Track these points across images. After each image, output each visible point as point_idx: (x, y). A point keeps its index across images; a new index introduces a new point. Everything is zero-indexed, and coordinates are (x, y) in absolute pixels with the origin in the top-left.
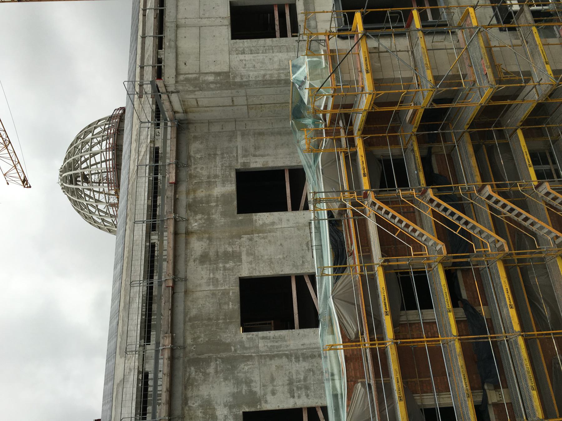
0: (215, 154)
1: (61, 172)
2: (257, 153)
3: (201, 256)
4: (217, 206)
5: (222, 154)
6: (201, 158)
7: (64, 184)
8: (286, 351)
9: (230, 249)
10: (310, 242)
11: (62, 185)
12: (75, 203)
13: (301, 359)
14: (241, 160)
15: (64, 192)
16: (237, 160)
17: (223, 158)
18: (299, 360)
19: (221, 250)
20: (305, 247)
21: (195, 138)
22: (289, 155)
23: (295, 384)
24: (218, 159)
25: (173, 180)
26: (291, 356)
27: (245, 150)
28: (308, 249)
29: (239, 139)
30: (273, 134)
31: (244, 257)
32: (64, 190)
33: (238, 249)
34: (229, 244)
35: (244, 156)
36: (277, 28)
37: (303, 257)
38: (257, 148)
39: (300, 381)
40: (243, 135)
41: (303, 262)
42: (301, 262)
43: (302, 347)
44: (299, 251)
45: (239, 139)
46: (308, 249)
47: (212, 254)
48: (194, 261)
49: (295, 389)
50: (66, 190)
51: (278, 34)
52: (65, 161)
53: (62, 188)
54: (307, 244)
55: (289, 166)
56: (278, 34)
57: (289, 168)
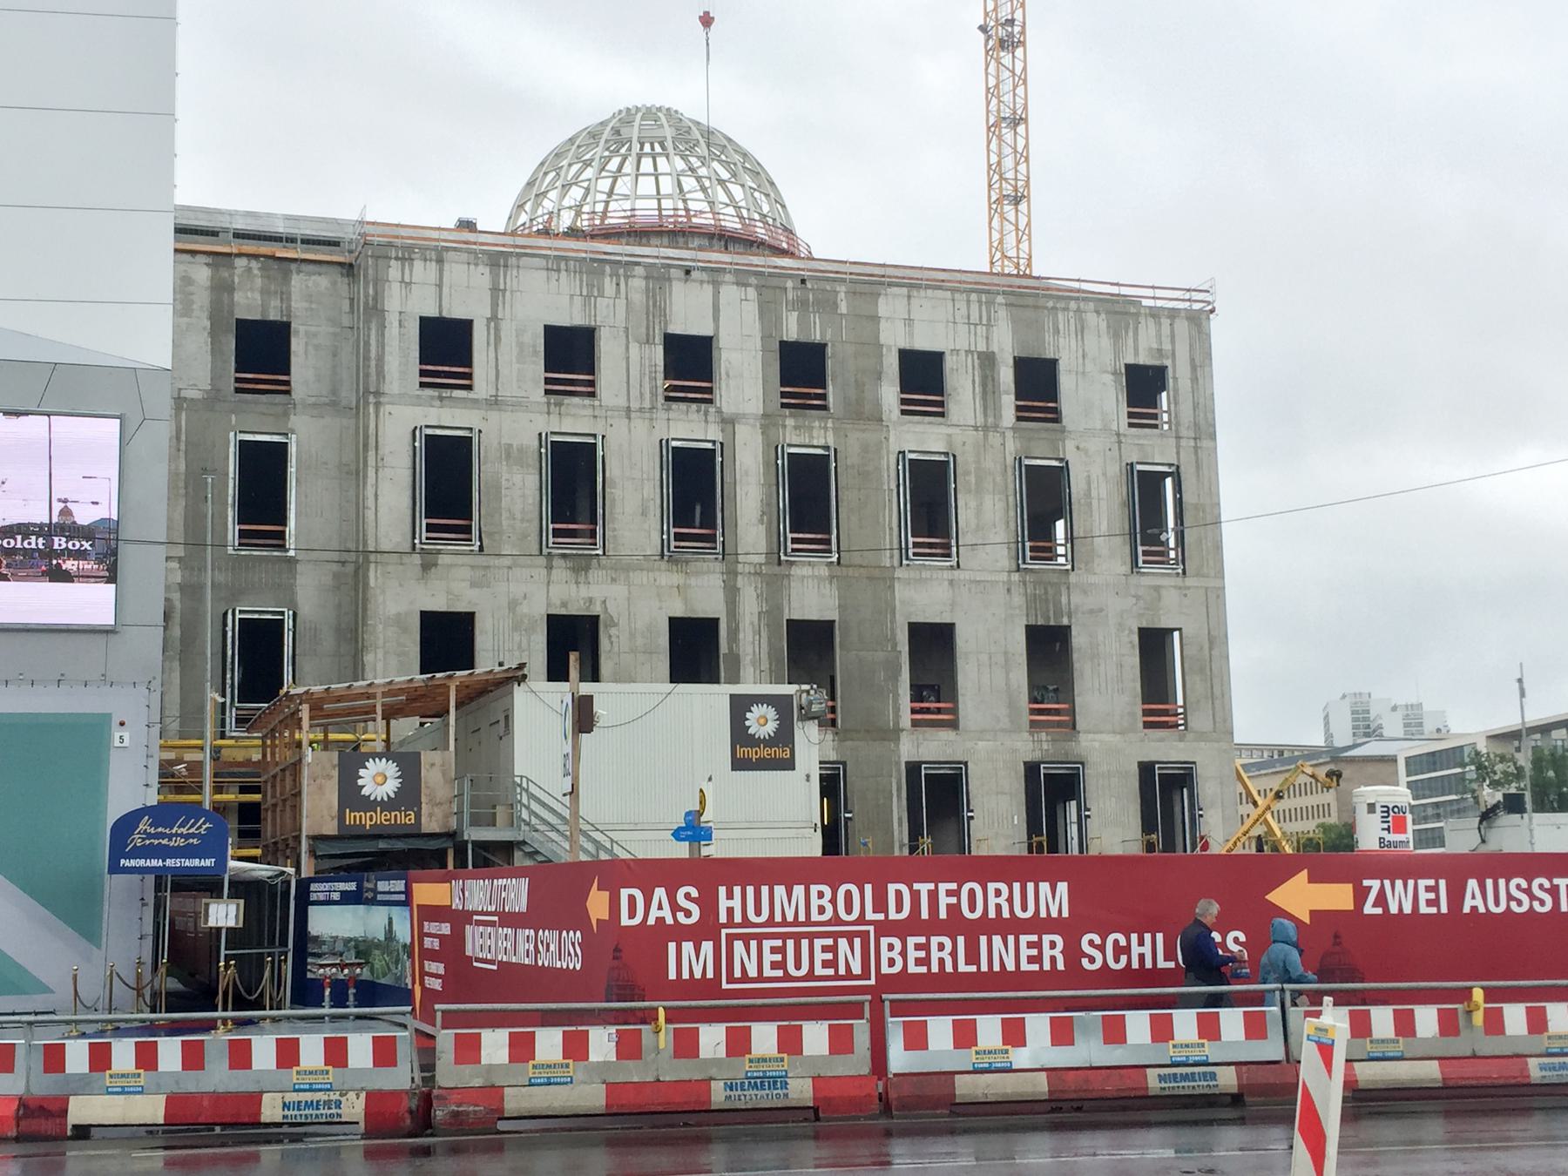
0: (311, 302)
1: (668, 109)
2: (310, 348)
3: (190, 278)
4: (247, 298)
5: (312, 309)
6: (307, 286)
7: (640, 115)
9: (195, 306)
11: (638, 109)
12: (593, 135)
14: (302, 329)
15: (620, 112)
16: (302, 325)
17: (306, 309)
19: (194, 297)
21: (334, 283)
24: (306, 305)
25: (278, 255)
27: (315, 335)
29: (331, 330)
30: (334, 367)
31: (185, 320)
32: (623, 114)
33: (194, 314)
34: (201, 307)
35: (306, 332)
36: (801, 536)
37: (181, 379)
38: (317, 347)
40: (335, 334)
45: (331, 330)
47: (191, 288)
48: (185, 271)
50: (627, 116)
51: (1146, 707)
52: (691, 120)
53: (628, 109)
54: (195, 385)
56: (1146, 707)
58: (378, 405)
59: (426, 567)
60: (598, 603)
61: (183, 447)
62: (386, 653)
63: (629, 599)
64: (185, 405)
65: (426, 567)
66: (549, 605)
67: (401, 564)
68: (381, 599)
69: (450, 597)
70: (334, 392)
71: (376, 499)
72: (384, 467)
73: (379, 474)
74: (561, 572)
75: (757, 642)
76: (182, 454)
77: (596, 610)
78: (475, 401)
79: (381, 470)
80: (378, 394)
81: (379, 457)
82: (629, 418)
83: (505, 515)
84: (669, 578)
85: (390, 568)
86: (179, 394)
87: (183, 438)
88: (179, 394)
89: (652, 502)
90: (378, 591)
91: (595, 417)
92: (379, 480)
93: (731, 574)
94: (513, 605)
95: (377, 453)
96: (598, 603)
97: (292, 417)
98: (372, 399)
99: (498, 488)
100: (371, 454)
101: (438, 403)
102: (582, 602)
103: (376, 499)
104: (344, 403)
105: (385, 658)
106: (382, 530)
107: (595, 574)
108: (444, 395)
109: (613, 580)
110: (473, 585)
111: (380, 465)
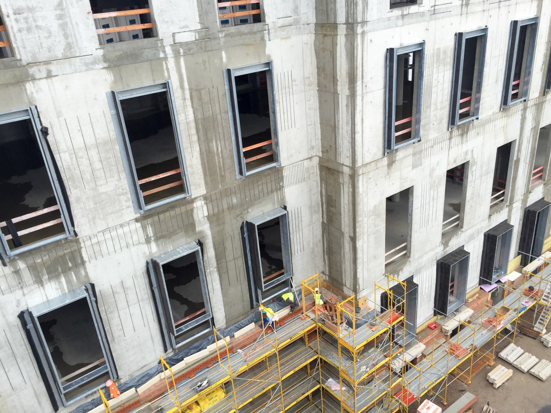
8: (66, 3)
10: (189, 30)
13: (61, 22)
18: (58, 19)
20: (183, 24)
22: (274, 3)
23: (30, 15)
26: (62, 9)
28: (181, 28)
39: (35, 20)
41: (167, 22)
42: (166, 20)
43: (74, 23)
44: (178, 16)
46: (181, 28)
49: (25, 15)
54: (186, 27)
55: (263, 4)
57: (261, 4)
58: (363, 33)
59: (391, 164)
60: (470, 153)
61: (188, 96)
62: (368, 236)
63: (483, 145)
64: (182, 51)
65: (391, 164)
66: (448, 164)
67: (377, 169)
68: (365, 200)
69: (402, 181)
70: (296, 9)
71: (362, 122)
72: (367, 93)
73: (364, 100)
74: (456, 139)
75: (527, 149)
76: (188, 102)
77: (469, 158)
78: (422, 14)
79: (365, 97)
80: (364, 23)
81: (364, 86)
82: (499, 8)
83: (433, 107)
84: (501, 122)
85: (371, 175)
86: (174, 40)
87: (186, 86)
88: (174, 40)
89: (501, 71)
90: (364, 195)
91: (484, 11)
92: (364, 106)
93: (525, 109)
94: (433, 170)
95: (362, 82)
96: (470, 153)
97: (268, 43)
98: (359, 30)
99: (431, 88)
100: (359, 83)
101: (400, 22)
102: (463, 156)
103: (362, 122)
104: (304, 19)
105: (368, 240)
106: (366, 148)
107: (471, 133)
108: (405, 12)
109: (478, 134)
110: (414, 166)
111: (364, 92)
